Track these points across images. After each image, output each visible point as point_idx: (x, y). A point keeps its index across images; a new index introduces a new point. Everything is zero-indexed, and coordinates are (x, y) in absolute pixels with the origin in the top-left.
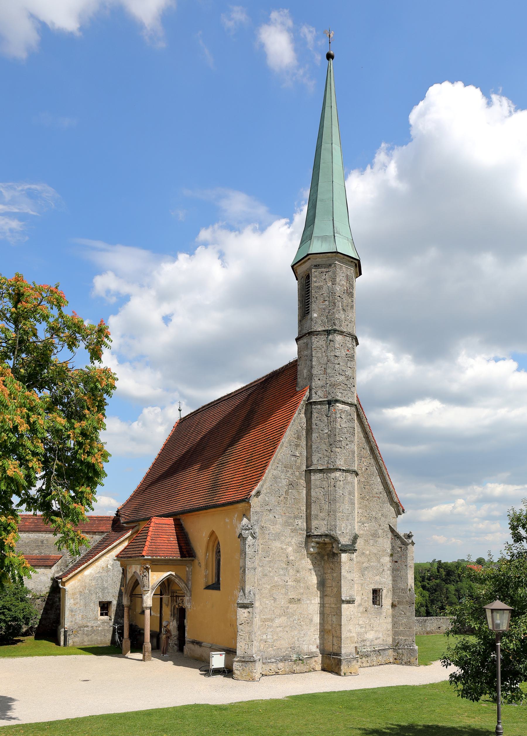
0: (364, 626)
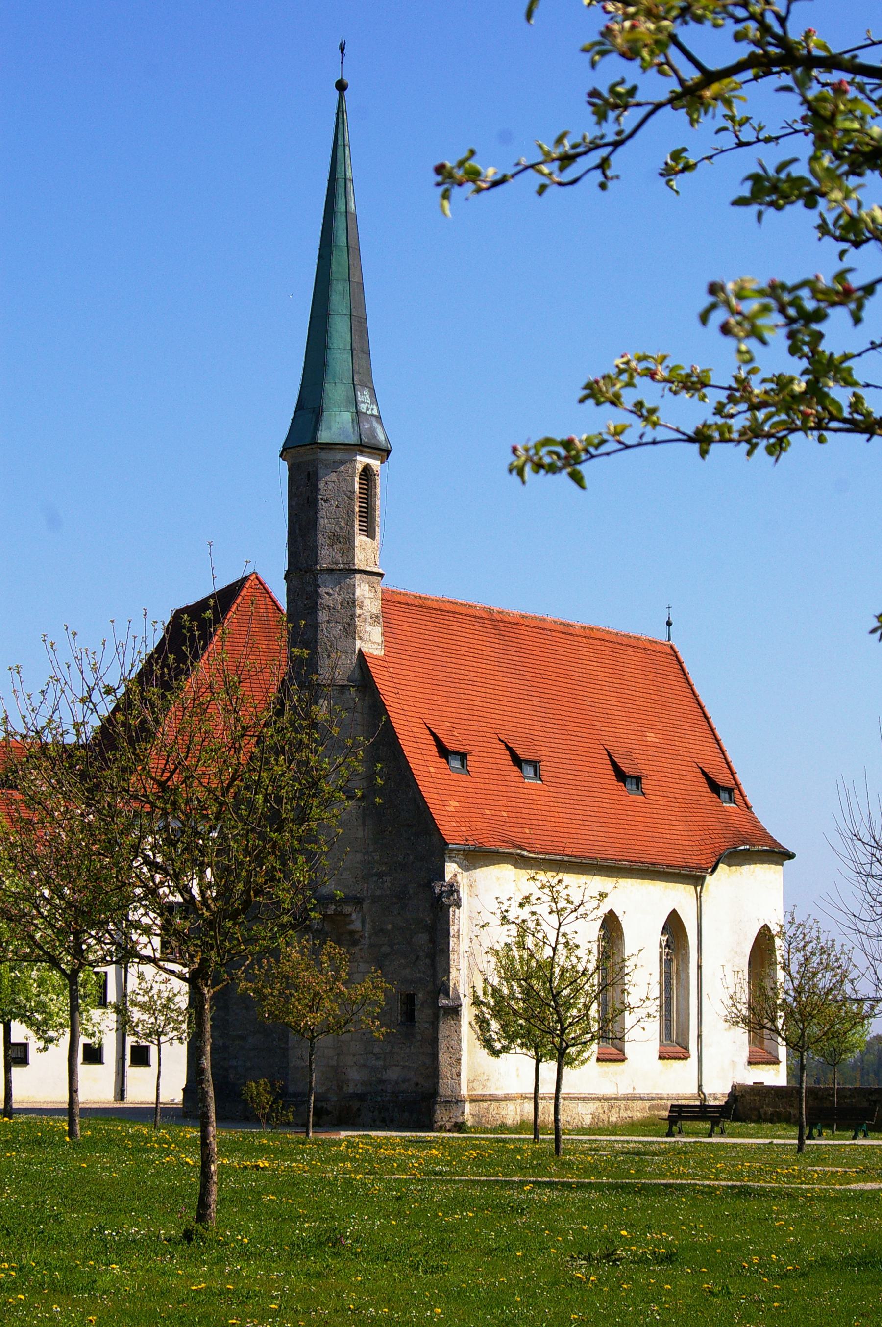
0: (383, 1056)
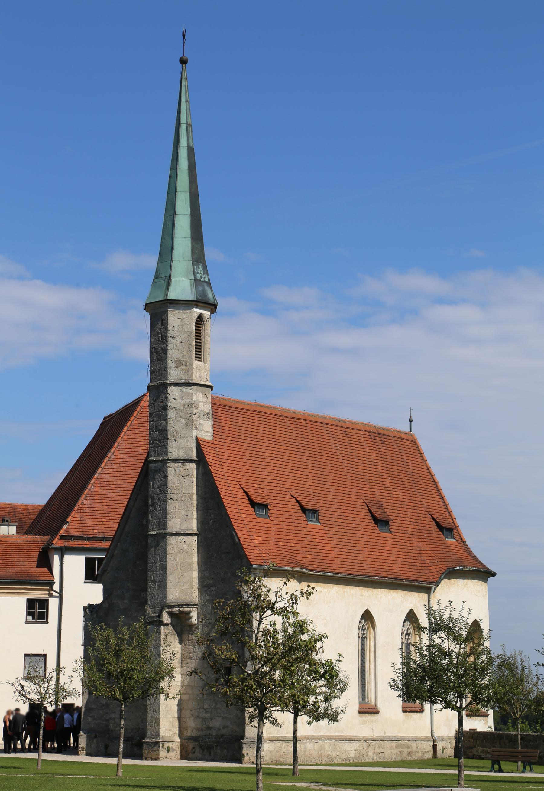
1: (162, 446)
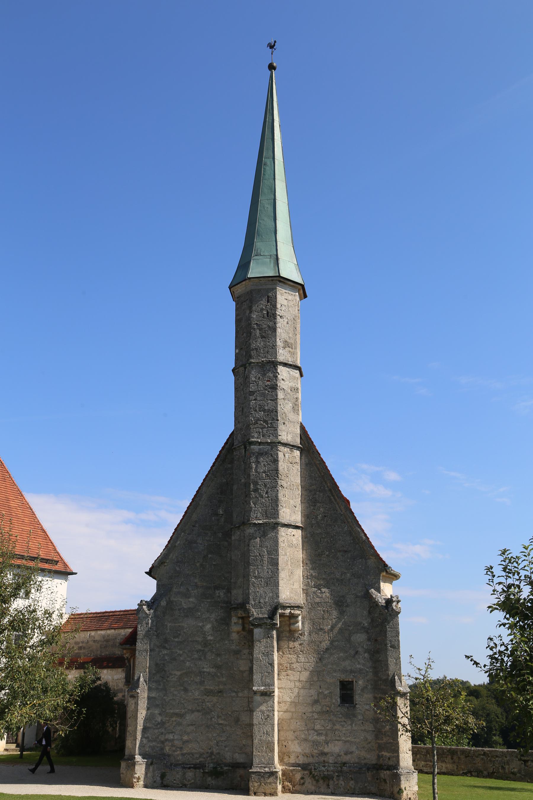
0: (324, 732)
1: (268, 427)
